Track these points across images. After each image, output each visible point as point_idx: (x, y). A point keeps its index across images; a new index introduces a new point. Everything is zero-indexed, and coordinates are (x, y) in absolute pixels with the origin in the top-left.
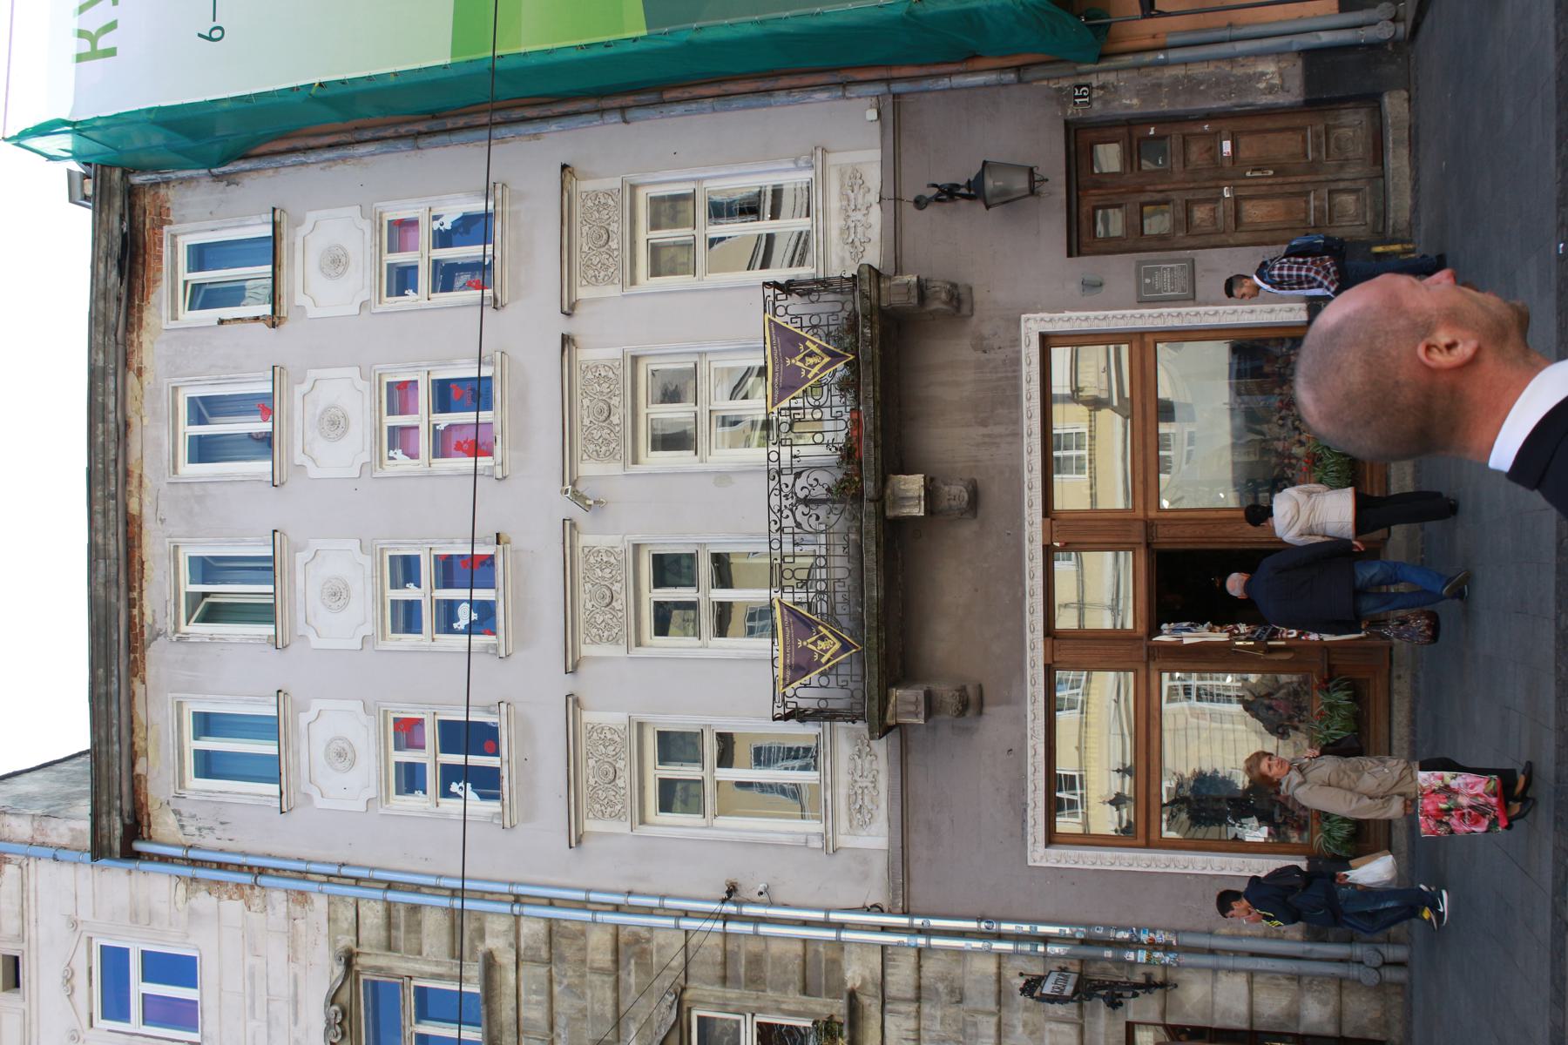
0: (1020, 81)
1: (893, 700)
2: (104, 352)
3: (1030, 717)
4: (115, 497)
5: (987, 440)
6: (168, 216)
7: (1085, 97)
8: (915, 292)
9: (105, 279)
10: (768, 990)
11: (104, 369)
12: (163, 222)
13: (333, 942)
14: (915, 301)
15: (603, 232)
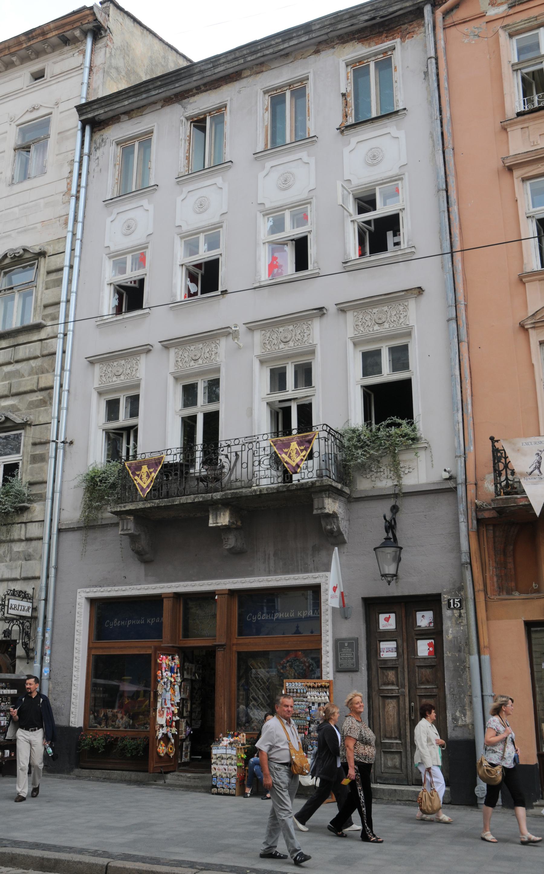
0: (462, 565)
1: (129, 518)
2: (321, 28)
3: (139, 587)
4: (245, 62)
5: (267, 556)
6: (408, 38)
7: (454, 606)
8: (319, 512)
9: (362, 13)
10: (30, 466)
11: (312, 31)
12: (403, 38)
13: (49, 243)
14: (315, 512)
15: (383, 320)
